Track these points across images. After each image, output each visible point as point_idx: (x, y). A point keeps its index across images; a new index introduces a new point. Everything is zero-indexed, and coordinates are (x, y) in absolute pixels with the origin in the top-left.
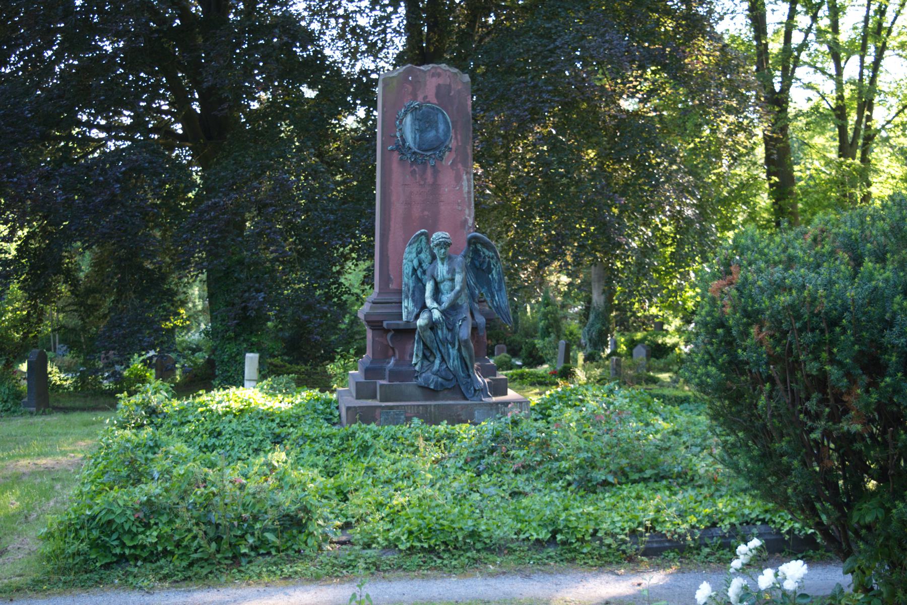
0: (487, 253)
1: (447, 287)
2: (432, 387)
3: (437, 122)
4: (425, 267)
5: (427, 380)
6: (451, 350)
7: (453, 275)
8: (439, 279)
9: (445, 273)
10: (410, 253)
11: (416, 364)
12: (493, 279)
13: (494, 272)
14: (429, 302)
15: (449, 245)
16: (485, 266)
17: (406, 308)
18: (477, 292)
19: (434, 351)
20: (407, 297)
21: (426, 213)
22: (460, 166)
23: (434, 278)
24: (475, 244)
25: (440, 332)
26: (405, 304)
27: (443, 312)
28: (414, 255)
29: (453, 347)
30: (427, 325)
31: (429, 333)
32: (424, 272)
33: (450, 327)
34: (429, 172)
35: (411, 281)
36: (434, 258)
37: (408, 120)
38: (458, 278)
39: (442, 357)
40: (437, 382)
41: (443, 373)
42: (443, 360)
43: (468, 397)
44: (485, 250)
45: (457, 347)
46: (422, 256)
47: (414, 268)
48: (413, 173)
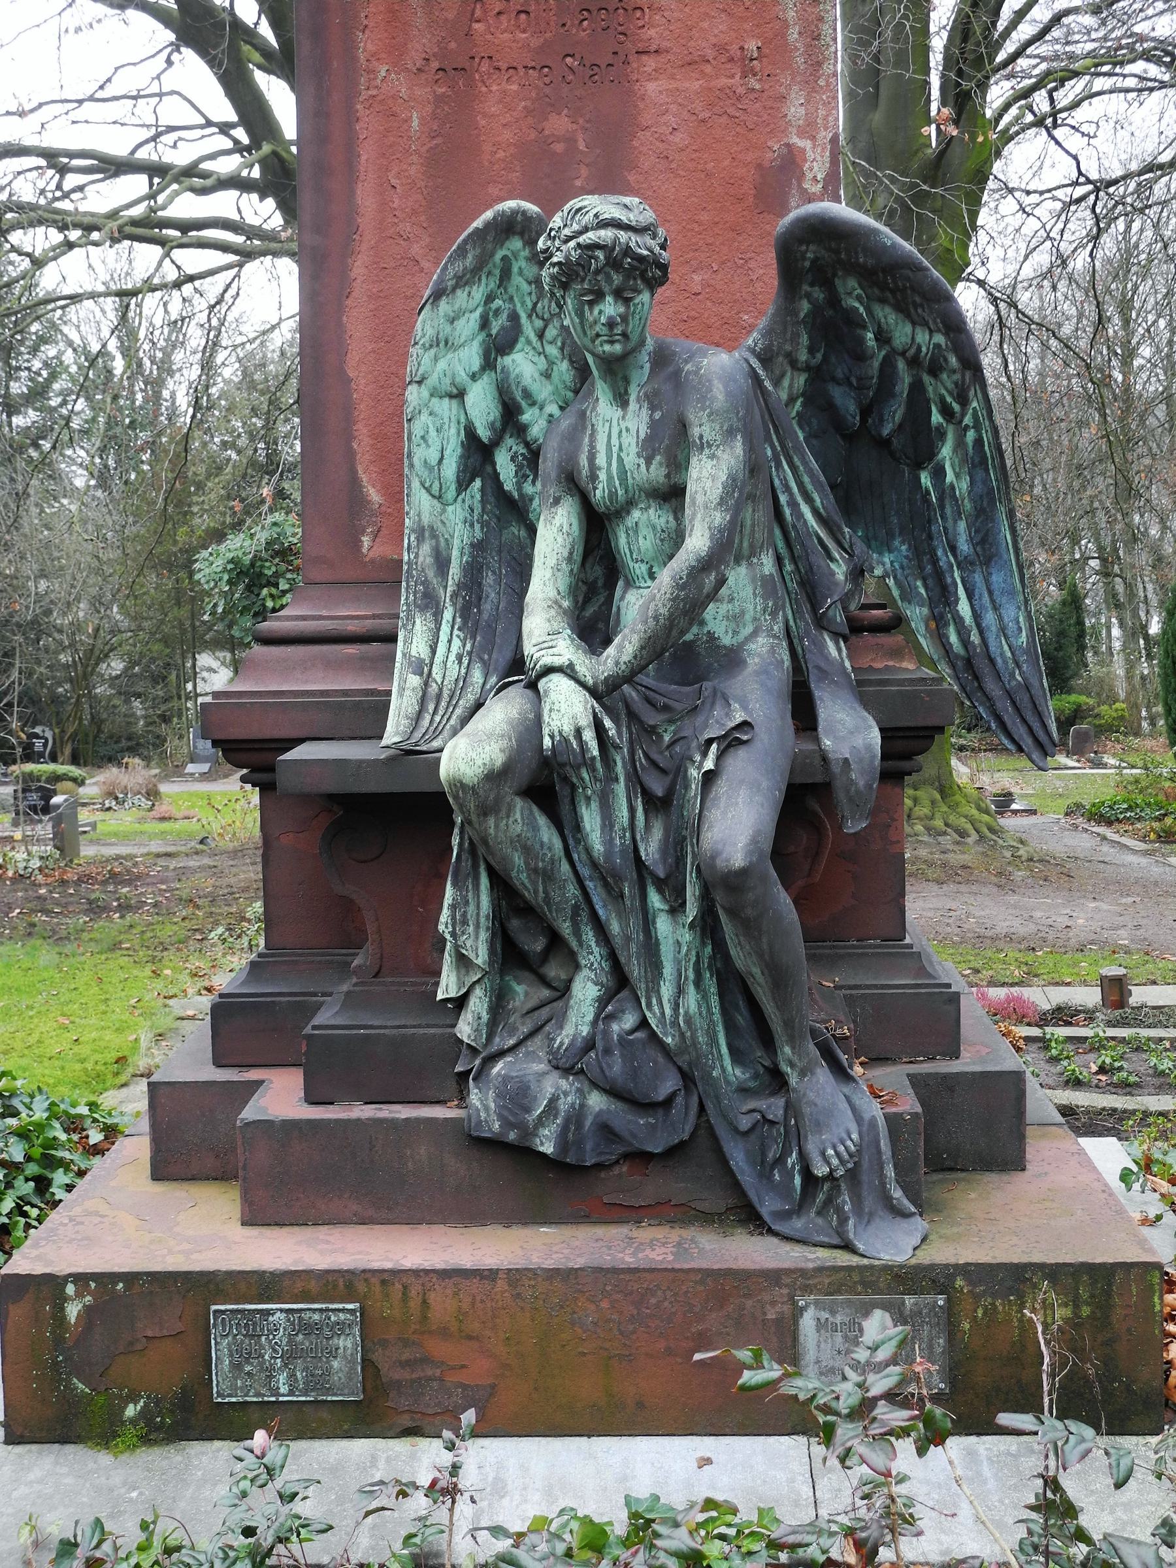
0: (902, 333)
1: (646, 543)
2: (548, 1148)
4: (536, 431)
5: (516, 1097)
6: (663, 926)
7: (678, 464)
8: (599, 494)
9: (631, 458)
10: (443, 344)
11: (460, 1002)
12: (946, 493)
13: (946, 451)
14: (544, 632)
15: (647, 273)
17: (421, 668)
18: (840, 570)
19: (565, 928)
20: (430, 603)
21: (559, 124)
23: (574, 485)
24: (823, 276)
25: (590, 819)
26: (414, 641)
27: (602, 693)
28: (471, 356)
29: (676, 909)
30: (494, 777)
31: (522, 825)
32: (533, 456)
33: (658, 789)
35: (456, 515)
36: (583, 373)
38: (709, 476)
39: (613, 957)
40: (576, 1117)
41: (616, 1067)
42: (619, 982)
43: (768, 1207)
44: (888, 316)
45: (692, 910)
46: (522, 364)
47: (470, 433)
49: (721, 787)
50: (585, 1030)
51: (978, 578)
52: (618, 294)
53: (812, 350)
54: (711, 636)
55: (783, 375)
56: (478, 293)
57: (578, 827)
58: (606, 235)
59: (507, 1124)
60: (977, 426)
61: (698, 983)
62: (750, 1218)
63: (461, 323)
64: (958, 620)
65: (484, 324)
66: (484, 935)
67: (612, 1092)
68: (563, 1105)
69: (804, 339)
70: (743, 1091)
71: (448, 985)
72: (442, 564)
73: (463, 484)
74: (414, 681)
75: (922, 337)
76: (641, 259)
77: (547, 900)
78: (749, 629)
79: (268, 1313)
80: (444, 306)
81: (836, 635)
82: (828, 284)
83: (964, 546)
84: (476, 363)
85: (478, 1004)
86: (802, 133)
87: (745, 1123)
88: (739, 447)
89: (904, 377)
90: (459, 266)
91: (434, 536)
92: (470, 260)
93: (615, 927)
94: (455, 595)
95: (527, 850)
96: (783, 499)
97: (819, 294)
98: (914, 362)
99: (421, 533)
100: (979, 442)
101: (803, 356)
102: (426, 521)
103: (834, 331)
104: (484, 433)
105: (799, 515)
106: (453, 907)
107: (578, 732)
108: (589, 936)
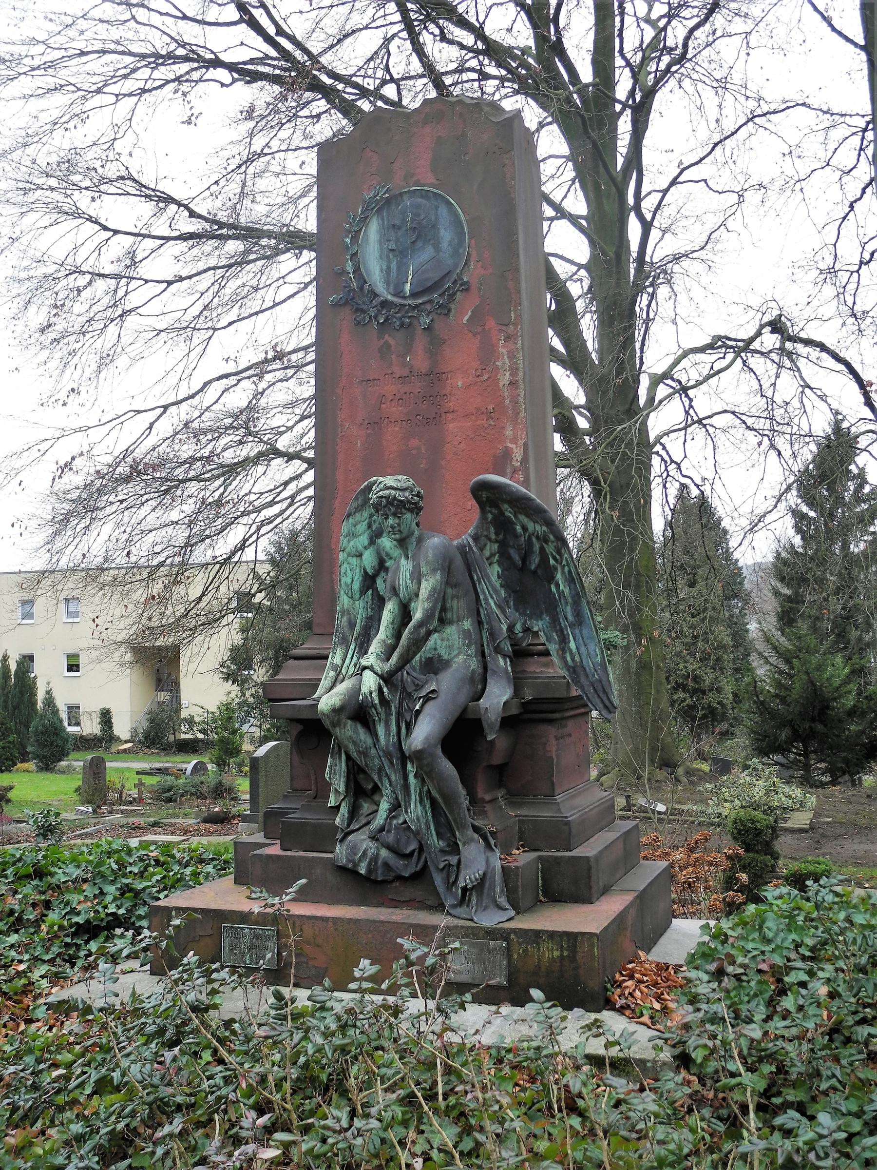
0: (531, 526)
2: (363, 872)
3: (434, 226)
10: (352, 535)
12: (561, 594)
13: (559, 576)
16: (535, 561)
20: (345, 642)
21: (415, 442)
22: (491, 323)
25: (381, 730)
28: (364, 539)
34: (421, 342)
37: (374, 229)
40: (375, 858)
43: (449, 902)
48: (384, 351)
49: (421, 717)
50: (382, 822)
51: (577, 631)
52: (395, 515)
53: (497, 534)
54: (439, 656)
55: (485, 545)
56: (366, 514)
57: (376, 735)
58: (387, 492)
59: (349, 861)
60: (568, 565)
61: (421, 802)
62: (440, 907)
63: (358, 527)
64: (571, 651)
65: (369, 526)
66: (342, 779)
67: (389, 848)
68: (369, 853)
69: (492, 530)
70: (443, 851)
71: (332, 802)
72: (352, 625)
73: (363, 592)
74: (332, 673)
75: (538, 528)
76: (401, 501)
77: (366, 765)
78: (456, 652)
79: (243, 929)
80: (351, 520)
81: (505, 656)
82: (497, 506)
83: (570, 618)
84: (366, 543)
85: (344, 810)
86: (511, 442)
87: (442, 865)
88: (438, 576)
89: (537, 546)
90: (356, 504)
91: (349, 614)
92: (360, 502)
93: (393, 778)
94: (357, 638)
95: (354, 743)
96: (482, 597)
97: (494, 511)
98: (538, 538)
99: (343, 612)
100: (570, 571)
101: (493, 537)
102: (346, 607)
103: (503, 526)
104: (370, 571)
105: (488, 604)
106: (331, 767)
107: (371, 693)
108: (386, 781)
